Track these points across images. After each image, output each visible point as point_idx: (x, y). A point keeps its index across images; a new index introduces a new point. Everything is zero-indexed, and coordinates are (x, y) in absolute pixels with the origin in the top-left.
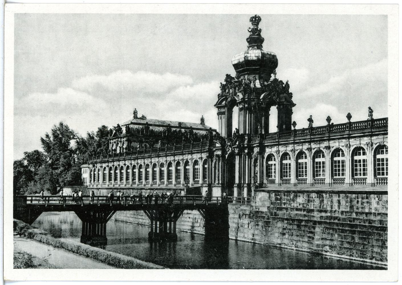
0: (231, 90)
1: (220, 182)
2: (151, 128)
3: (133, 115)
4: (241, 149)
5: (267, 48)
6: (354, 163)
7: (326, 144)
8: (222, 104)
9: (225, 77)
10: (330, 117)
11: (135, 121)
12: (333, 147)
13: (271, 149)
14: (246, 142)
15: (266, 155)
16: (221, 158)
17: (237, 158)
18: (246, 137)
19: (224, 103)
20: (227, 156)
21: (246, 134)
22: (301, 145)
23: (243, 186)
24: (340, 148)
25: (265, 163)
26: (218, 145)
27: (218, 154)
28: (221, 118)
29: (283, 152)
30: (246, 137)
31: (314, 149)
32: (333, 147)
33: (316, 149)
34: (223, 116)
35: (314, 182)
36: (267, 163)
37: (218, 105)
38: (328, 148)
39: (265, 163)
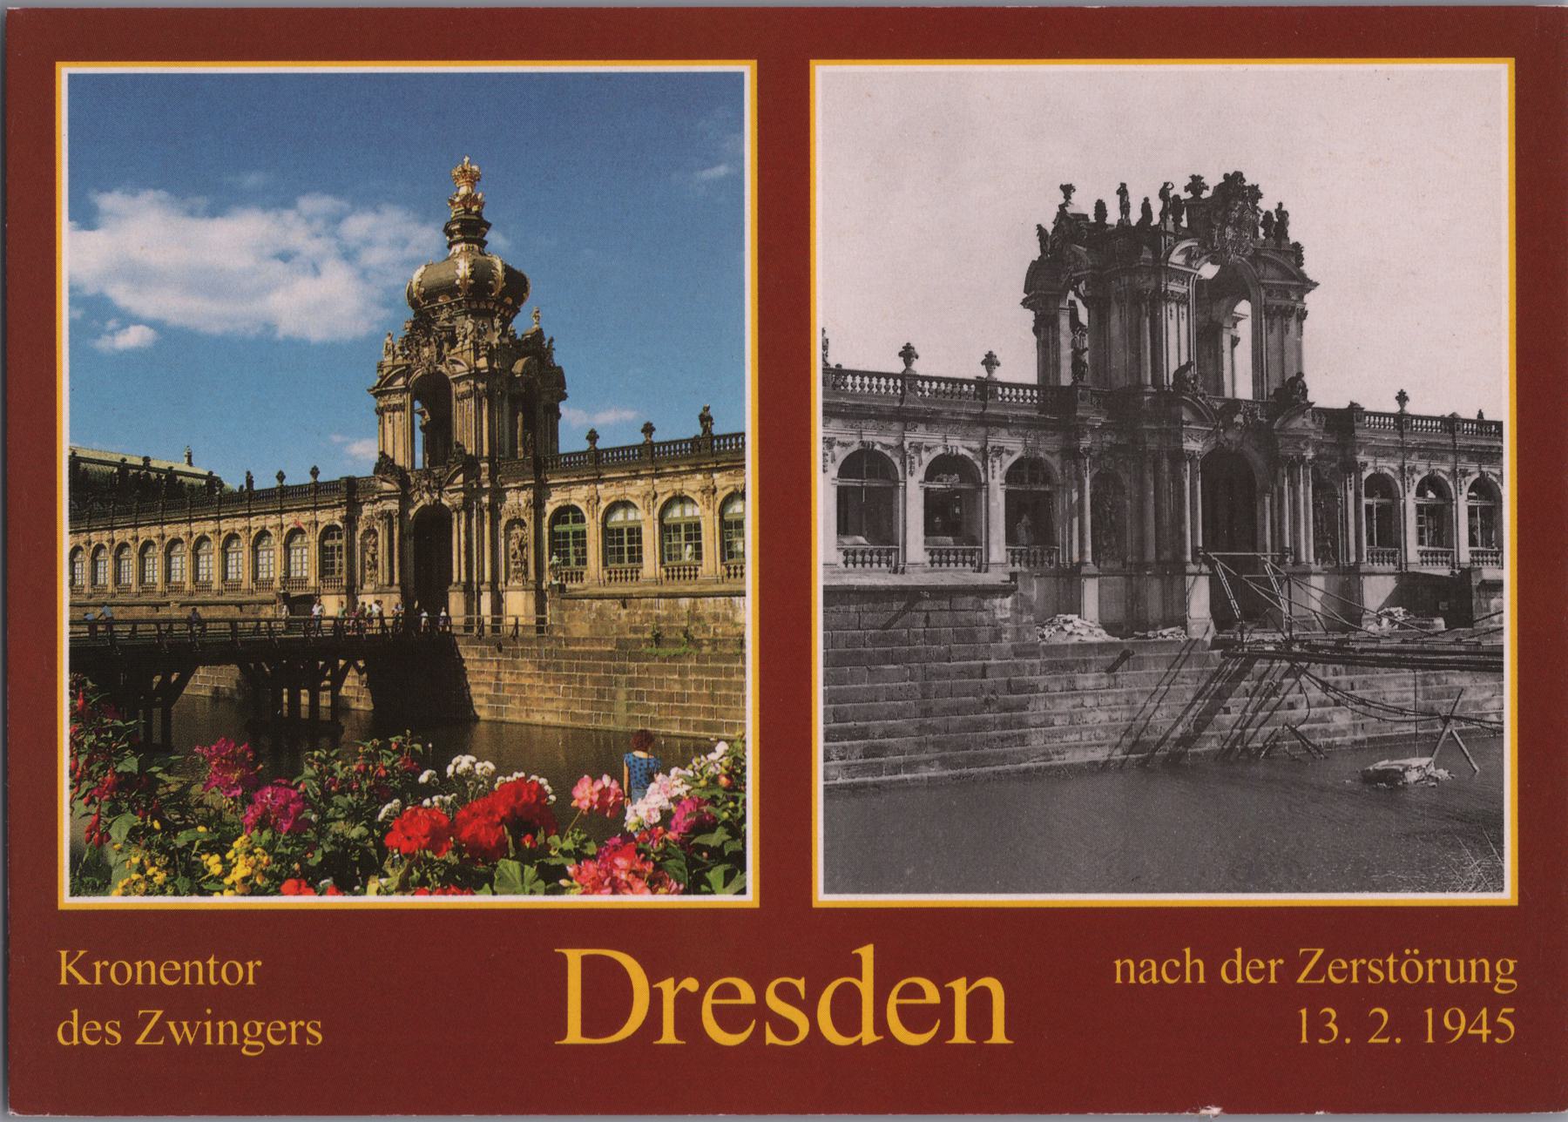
1: (396, 580)
4: (471, 494)
5: (500, 249)
6: (666, 530)
14: (484, 476)
15: (549, 509)
16: (396, 520)
18: (484, 465)
20: (412, 512)
21: (481, 457)
23: (478, 588)
25: (546, 530)
27: (390, 511)
30: (484, 465)
36: (551, 527)
39: (546, 530)
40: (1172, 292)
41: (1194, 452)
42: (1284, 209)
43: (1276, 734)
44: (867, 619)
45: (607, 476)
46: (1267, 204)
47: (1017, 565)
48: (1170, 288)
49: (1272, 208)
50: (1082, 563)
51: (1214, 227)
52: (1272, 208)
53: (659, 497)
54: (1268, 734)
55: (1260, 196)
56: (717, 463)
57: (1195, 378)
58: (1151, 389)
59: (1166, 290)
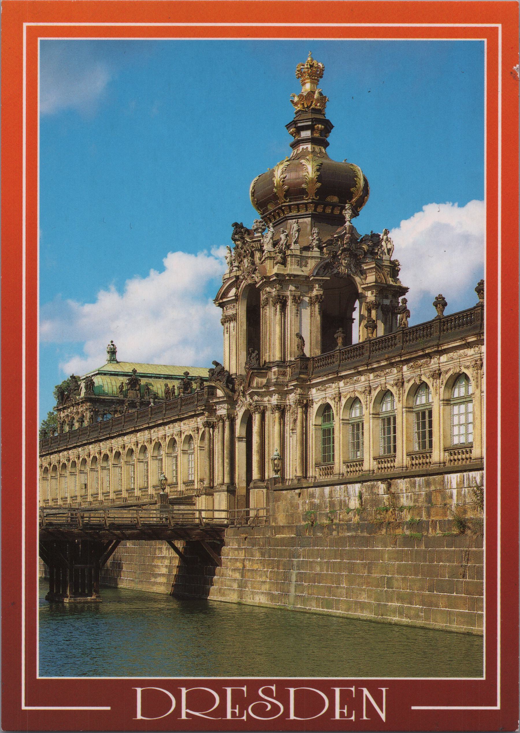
0: (245, 260)
2: (143, 382)
3: (108, 356)
7: (434, 363)
8: (229, 296)
9: (233, 228)
10: (444, 299)
11: (112, 368)
12: (447, 372)
13: (324, 393)
17: (257, 418)
19: (233, 292)
22: (383, 374)
24: (462, 371)
26: (220, 393)
27: (221, 415)
28: (227, 331)
29: (348, 397)
31: (409, 381)
32: (447, 372)
33: (412, 382)
34: (232, 324)
35: (410, 463)
37: (221, 298)
38: (437, 374)
45: (343, 374)
53: (373, 392)
56: (423, 350)
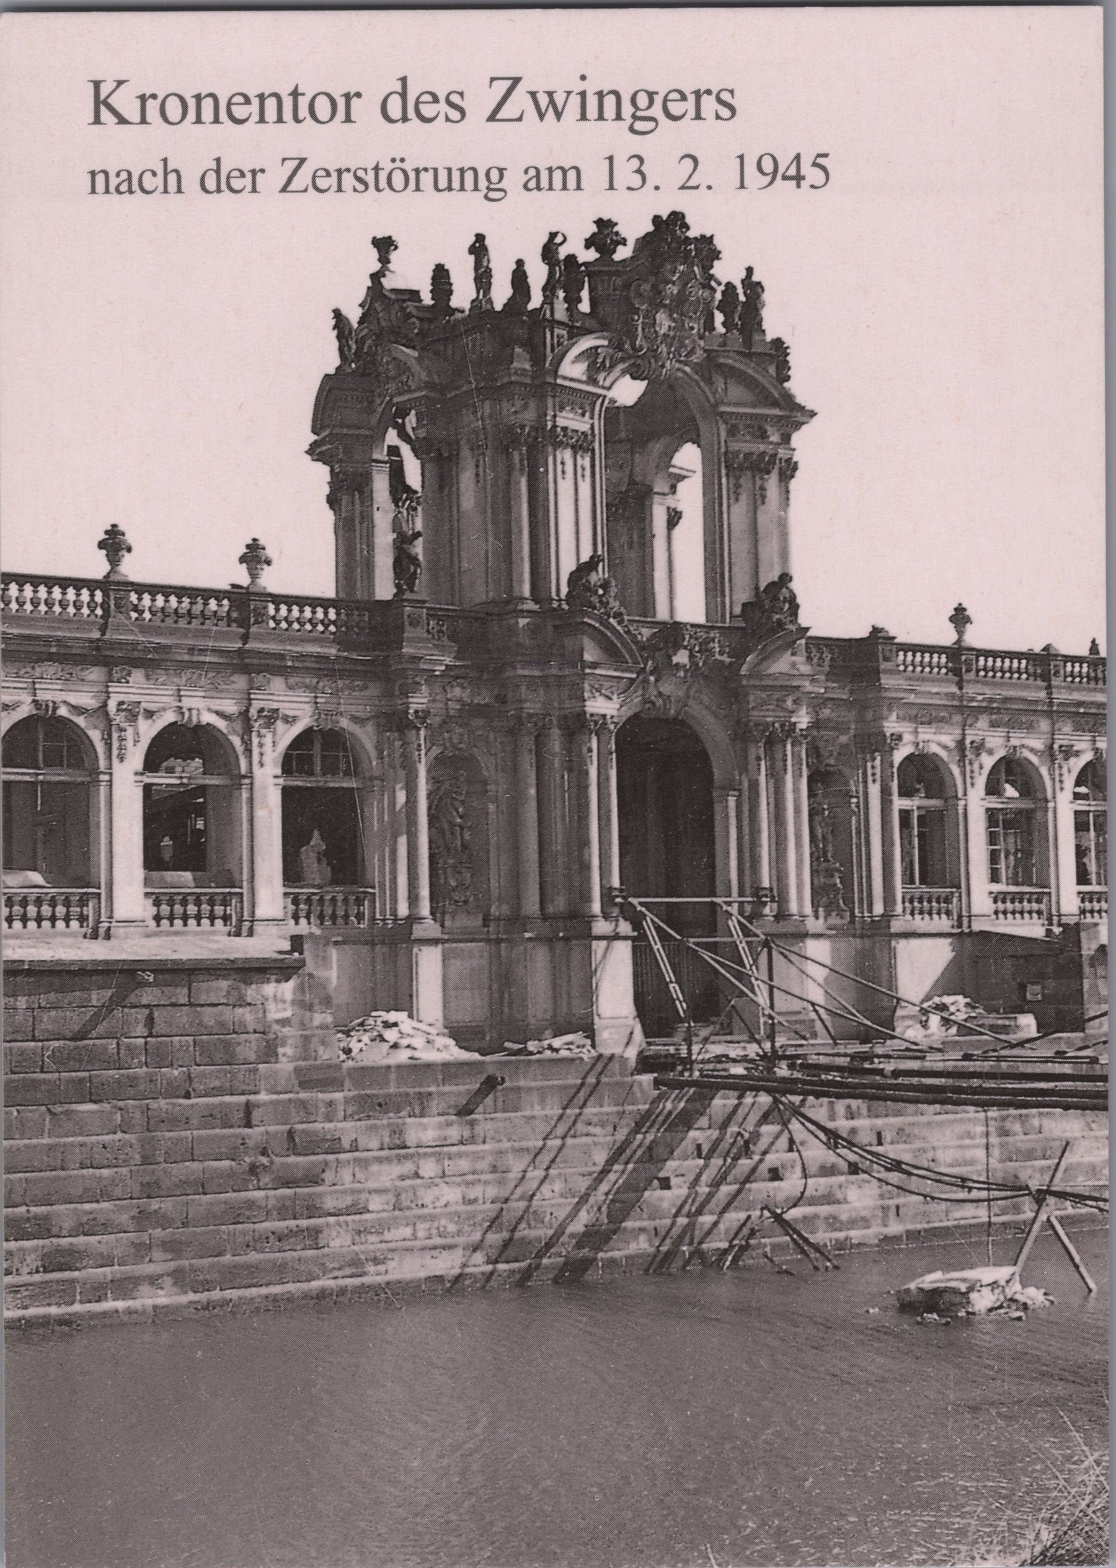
40: (565, 429)
41: (604, 716)
42: (756, 278)
43: (749, 1225)
44: (48, 1021)
46: (727, 271)
47: (303, 921)
48: (561, 422)
49: (736, 277)
50: (413, 919)
51: (636, 311)
52: (736, 277)
54: (735, 1225)
55: (716, 255)
57: (605, 585)
58: (531, 606)
59: (555, 426)
